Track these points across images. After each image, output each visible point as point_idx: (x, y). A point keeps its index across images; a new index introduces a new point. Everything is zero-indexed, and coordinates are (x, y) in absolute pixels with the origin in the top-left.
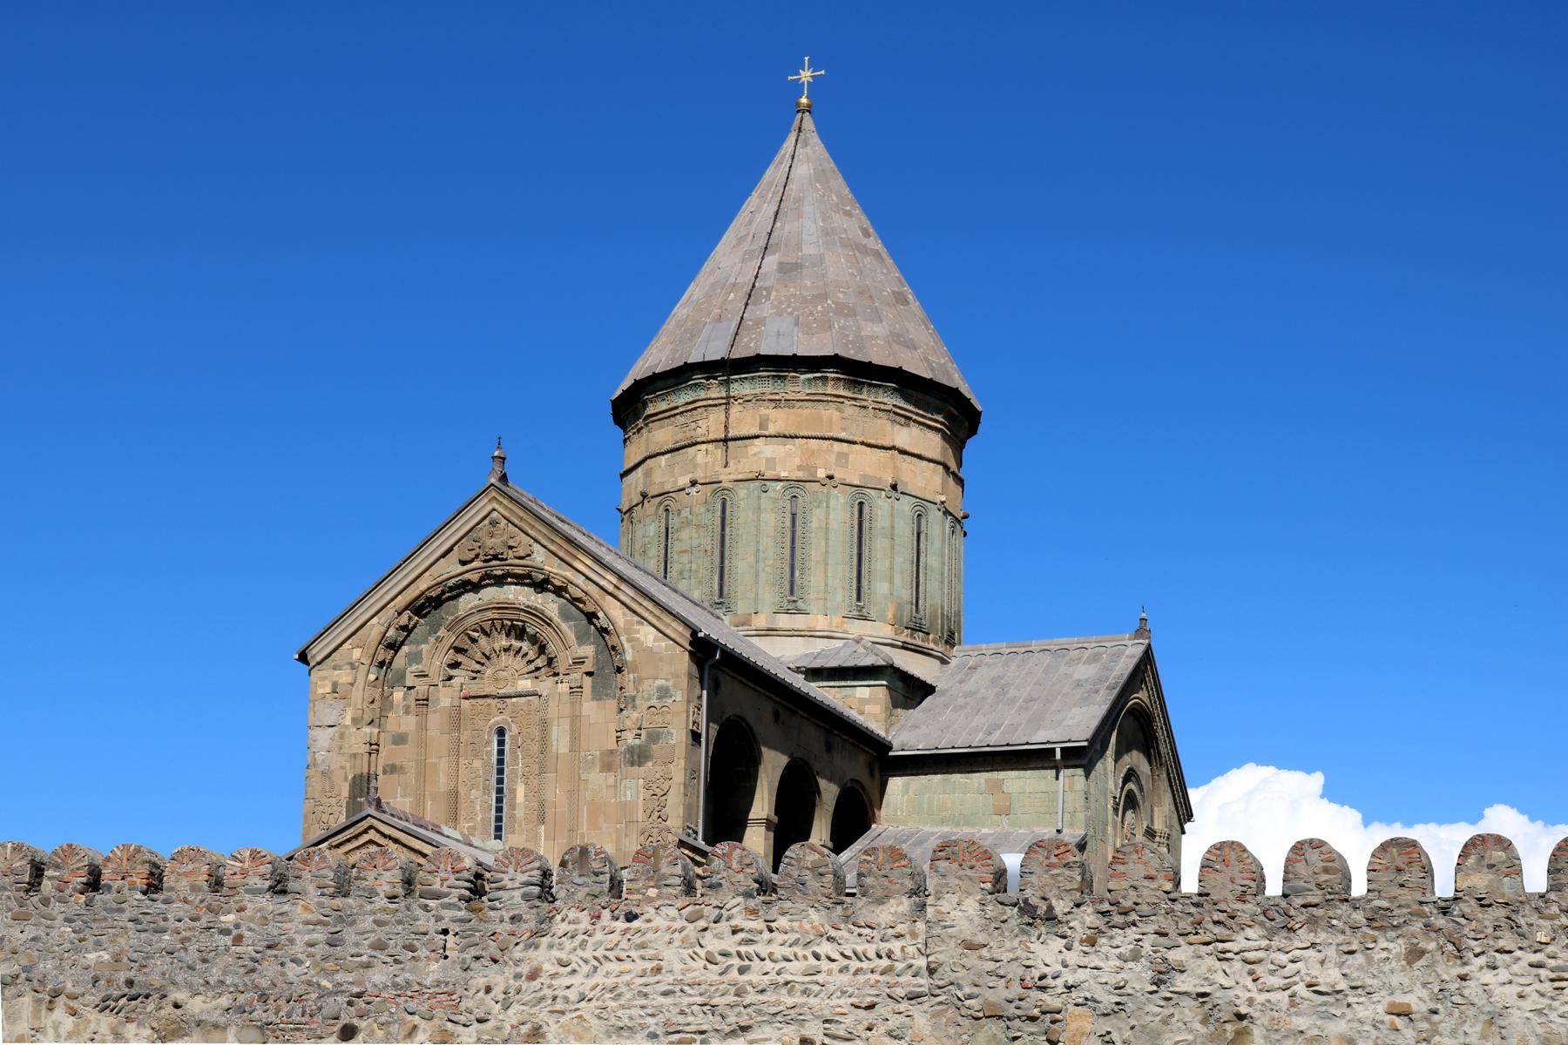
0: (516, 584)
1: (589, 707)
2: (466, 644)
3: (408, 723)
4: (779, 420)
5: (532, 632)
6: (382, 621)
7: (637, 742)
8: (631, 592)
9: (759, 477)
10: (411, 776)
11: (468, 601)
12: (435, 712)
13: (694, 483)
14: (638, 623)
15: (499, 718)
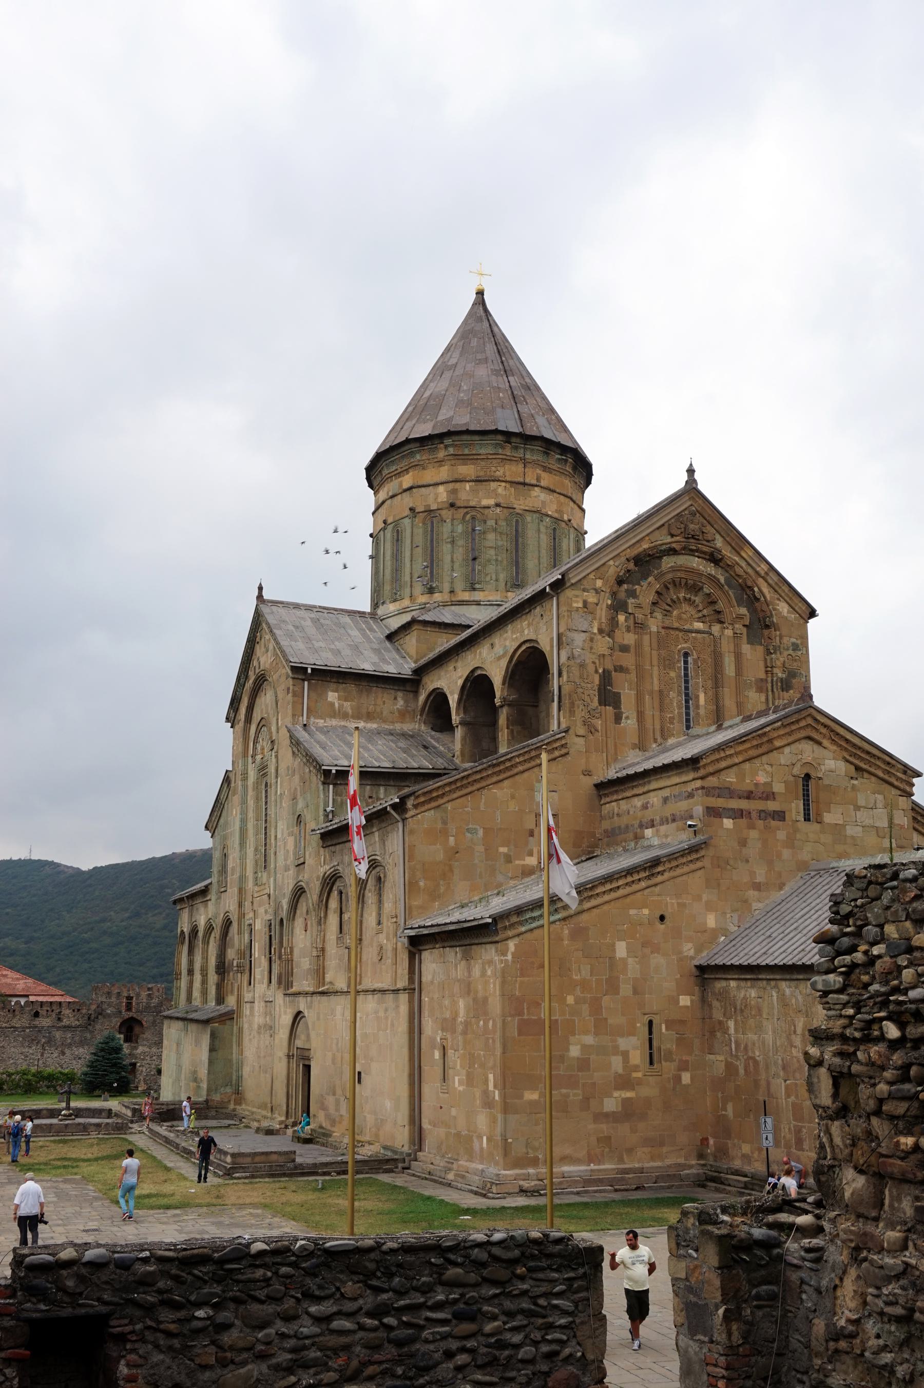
0: (699, 557)
1: (746, 648)
2: (664, 591)
3: (629, 639)
4: (547, 479)
5: (708, 592)
6: (617, 564)
7: (784, 676)
8: (776, 578)
9: (540, 514)
10: (633, 676)
11: (668, 562)
12: (646, 634)
13: (498, 505)
14: (779, 599)
15: (685, 645)
